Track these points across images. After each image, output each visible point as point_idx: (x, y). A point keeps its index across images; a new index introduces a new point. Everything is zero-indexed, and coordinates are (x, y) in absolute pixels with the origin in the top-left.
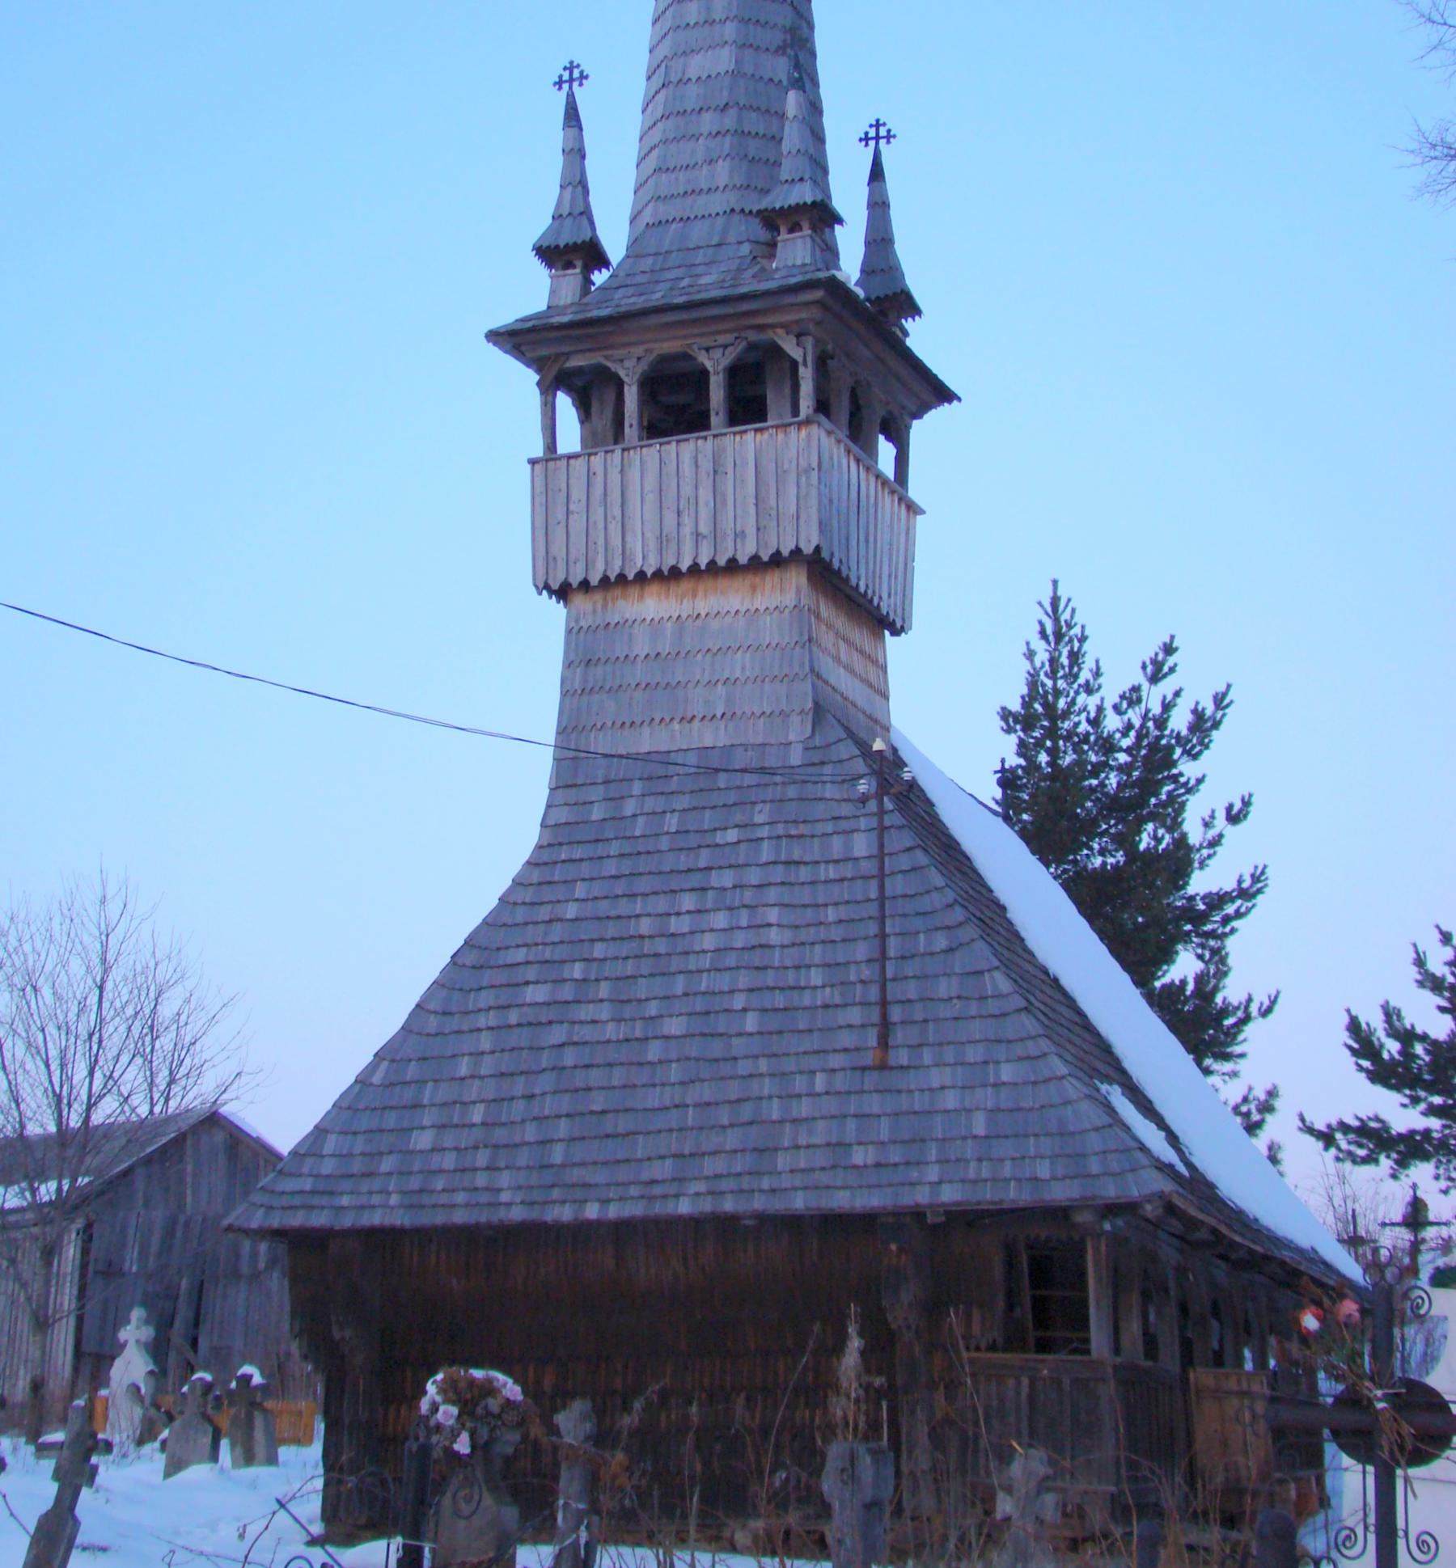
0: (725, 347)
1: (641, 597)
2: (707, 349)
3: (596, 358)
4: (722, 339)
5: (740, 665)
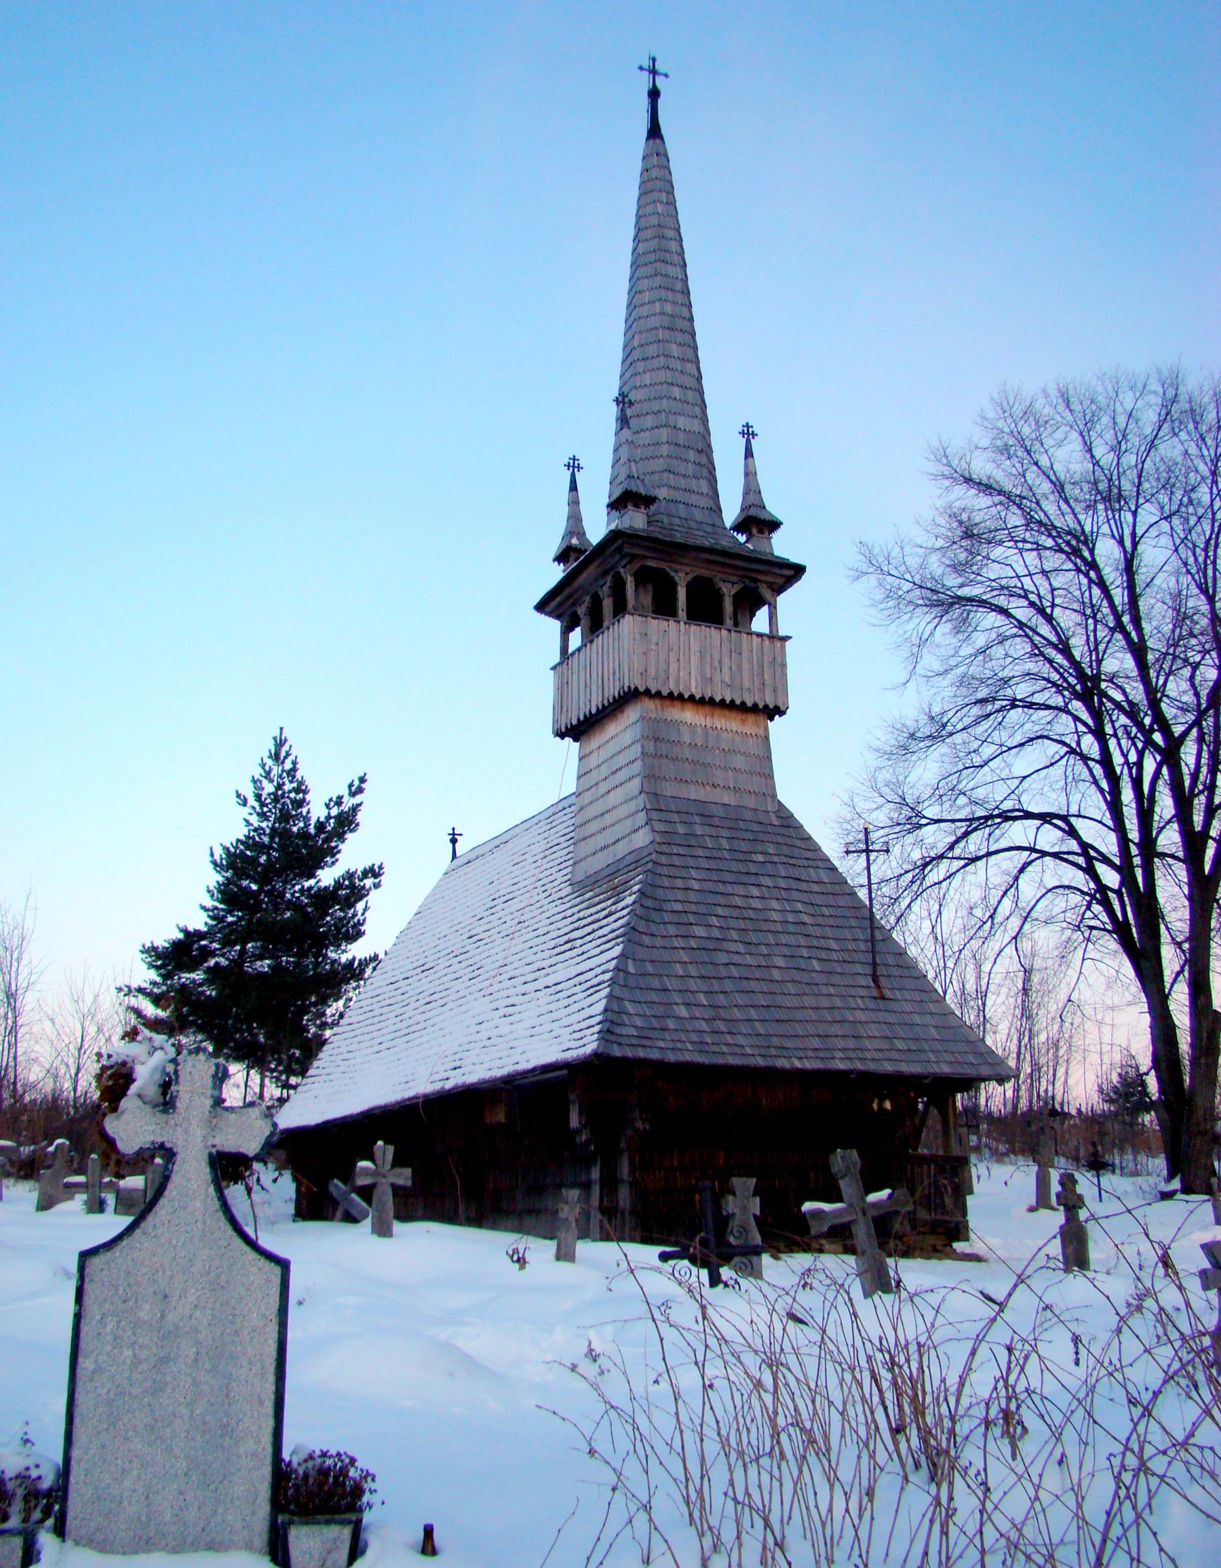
0: (733, 583)
1: (683, 709)
2: (724, 581)
3: (664, 565)
4: (732, 579)
5: (739, 762)
